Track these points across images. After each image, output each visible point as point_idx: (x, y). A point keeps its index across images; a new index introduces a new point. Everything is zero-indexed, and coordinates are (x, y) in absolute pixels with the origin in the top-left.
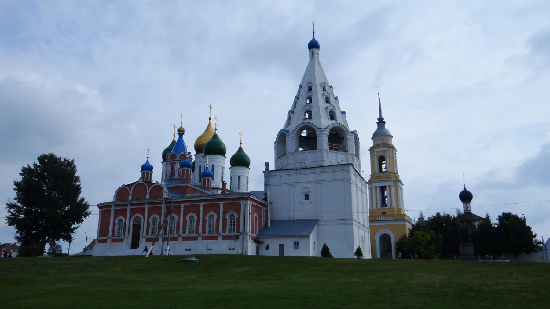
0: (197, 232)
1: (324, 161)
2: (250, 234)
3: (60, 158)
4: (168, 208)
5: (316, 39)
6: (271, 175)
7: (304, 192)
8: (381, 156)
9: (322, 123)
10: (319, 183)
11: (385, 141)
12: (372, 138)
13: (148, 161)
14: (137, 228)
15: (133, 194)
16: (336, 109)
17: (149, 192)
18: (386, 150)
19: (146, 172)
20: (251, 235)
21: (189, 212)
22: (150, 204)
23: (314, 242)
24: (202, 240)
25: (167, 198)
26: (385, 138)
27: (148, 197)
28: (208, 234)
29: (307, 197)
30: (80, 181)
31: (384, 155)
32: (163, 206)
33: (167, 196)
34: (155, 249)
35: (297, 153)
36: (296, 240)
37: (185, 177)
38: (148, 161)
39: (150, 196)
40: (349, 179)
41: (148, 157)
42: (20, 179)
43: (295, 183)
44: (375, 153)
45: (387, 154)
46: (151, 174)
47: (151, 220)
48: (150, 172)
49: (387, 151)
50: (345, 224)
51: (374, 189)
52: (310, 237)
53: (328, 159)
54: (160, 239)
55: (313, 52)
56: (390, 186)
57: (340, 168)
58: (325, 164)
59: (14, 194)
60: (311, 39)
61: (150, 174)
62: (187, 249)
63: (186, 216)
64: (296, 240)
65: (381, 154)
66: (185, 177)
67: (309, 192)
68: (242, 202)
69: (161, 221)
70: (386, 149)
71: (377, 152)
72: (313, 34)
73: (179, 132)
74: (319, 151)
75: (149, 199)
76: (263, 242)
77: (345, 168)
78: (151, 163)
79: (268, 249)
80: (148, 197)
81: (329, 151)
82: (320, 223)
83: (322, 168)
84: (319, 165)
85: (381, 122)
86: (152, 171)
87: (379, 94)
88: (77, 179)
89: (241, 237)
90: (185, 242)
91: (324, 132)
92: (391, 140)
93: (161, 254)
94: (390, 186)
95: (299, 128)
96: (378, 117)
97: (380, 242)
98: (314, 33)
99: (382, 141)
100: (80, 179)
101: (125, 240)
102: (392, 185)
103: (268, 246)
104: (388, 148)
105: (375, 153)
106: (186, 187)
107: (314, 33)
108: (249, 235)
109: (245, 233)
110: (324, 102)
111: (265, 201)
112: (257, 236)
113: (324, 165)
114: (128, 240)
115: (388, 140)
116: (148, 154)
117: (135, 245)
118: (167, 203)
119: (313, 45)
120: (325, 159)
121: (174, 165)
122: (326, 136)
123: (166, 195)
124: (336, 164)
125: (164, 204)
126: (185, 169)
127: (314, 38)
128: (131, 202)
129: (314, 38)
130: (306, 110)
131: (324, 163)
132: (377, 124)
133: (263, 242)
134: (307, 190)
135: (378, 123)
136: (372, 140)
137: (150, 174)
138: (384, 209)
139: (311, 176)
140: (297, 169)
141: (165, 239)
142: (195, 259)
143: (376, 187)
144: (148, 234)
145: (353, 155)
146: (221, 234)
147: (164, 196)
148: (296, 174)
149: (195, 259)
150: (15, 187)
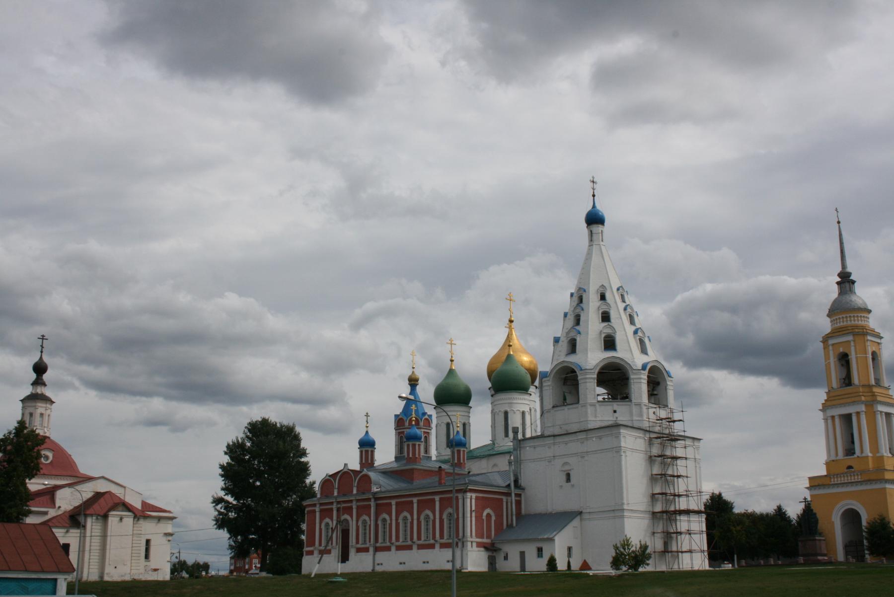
0: (412, 539)
1: (589, 422)
2: (475, 539)
3: (274, 423)
4: (377, 505)
5: (598, 207)
6: (522, 446)
7: (564, 471)
8: (841, 353)
9: (589, 360)
10: (582, 455)
11: (849, 322)
12: (828, 316)
13: (367, 432)
14: (345, 534)
15: (339, 488)
16: (615, 331)
17: (356, 485)
18: (849, 342)
19: (364, 449)
20: (475, 542)
21: (402, 511)
22: (358, 501)
23: (570, 549)
24: (419, 549)
25: (376, 493)
26: (848, 315)
27: (355, 492)
28: (425, 540)
29: (568, 478)
30: (307, 455)
31: (847, 351)
32: (372, 503)
33: (377, 488)
34: (360, 563)
35: (555, 411)
36: (540, 545)
37: (411, 456)
38: (367, 432)
39: (358, 490)
40: (619, 448)
41: (367, 427)
42: (226, 459)
43: (552, 458)
44: (831, 348)
45: (853, 348)
46: (373, 452)
47: (360, 523)
48: (370, 449)
49: (852, 344)
50: (614, 517)
51: (830, 421)
52: (554, 540)
53: (596, 417)
54: (371, 550)
55: (591, 231)
56: (858, 413)
57: (607, 432)
58: (590, 426)
59: (220, 483)
60: (590, 208)
61: (370, 452)
62: (401, 561)
63: (399, 517)
64: (540, 545)
65: (841, 350)
66: (411, 456)
67: (570, 470)
68: (460, 496)
69: (370, 524)
70: (850, 338)
71: (833, 345)
72: (593, 198)
73: (411, 383)
74: (582, 406)
75: (356, 494)
76: (500, 549)
77: (615, 431)
78: (373, 435)
79: (507, 559)
80: (355, 492)
81: (597, 405)
82: (585, 516)
83: (585, 433)
84: (582, 429)
85: (846, 281)
86: (375, 447)
87: (839, 222)
88: (304, 453)
89: (460, 544)
90: (400, 553)
91: (588, 376)
92: (868, 318)
93: (373, 570)
94: (858, 413)
95: (556, 372)
96: (839, 269)
97: (844, 526)
98: (594, 196)
99: (851, 321)
100: (307, 452)
101: (333, 551)
102: (863, 411)
103: (507, 554)
104: (853, 335)
105: (831, 348)
106: (412, 470)
107: (594, 196)
108: (472, 542)
109: (465, 540)
110: (599, 321)
111: (507, 489)
112: (492, 541)
113: (590, 428)
114: (336, 552)
115: (863, 319)
116: (367, 421)
117: (344, 558)
118: (376, 499)
119: (594, 219)
120: (591, 418)
121: (402, 435)
122: (592, 380)
123: (375, 488)
124: (610, 423)
125: (373, 500)
126: (411, 443)
127: (594, 206)
128: (336, 499)
129: (594, 206)
130: (571, 338)
131: (589, 425)
132: (836, 285)
133: (500, 549)
134: (567, 468)
135: (838, 283)
136: (828, 320)
137: (370, 452)
138: (850, 461)
139: (574, 446)
140: (554, 436)
141: (377, 549)
142: (342, 580)
143: (833, 417)
144: (357, 542)
145: (640, 404)
146: (438, 540)
147: (372, 489)
148: (554, 444)
149: (342, 580)
150: (220, 471)
